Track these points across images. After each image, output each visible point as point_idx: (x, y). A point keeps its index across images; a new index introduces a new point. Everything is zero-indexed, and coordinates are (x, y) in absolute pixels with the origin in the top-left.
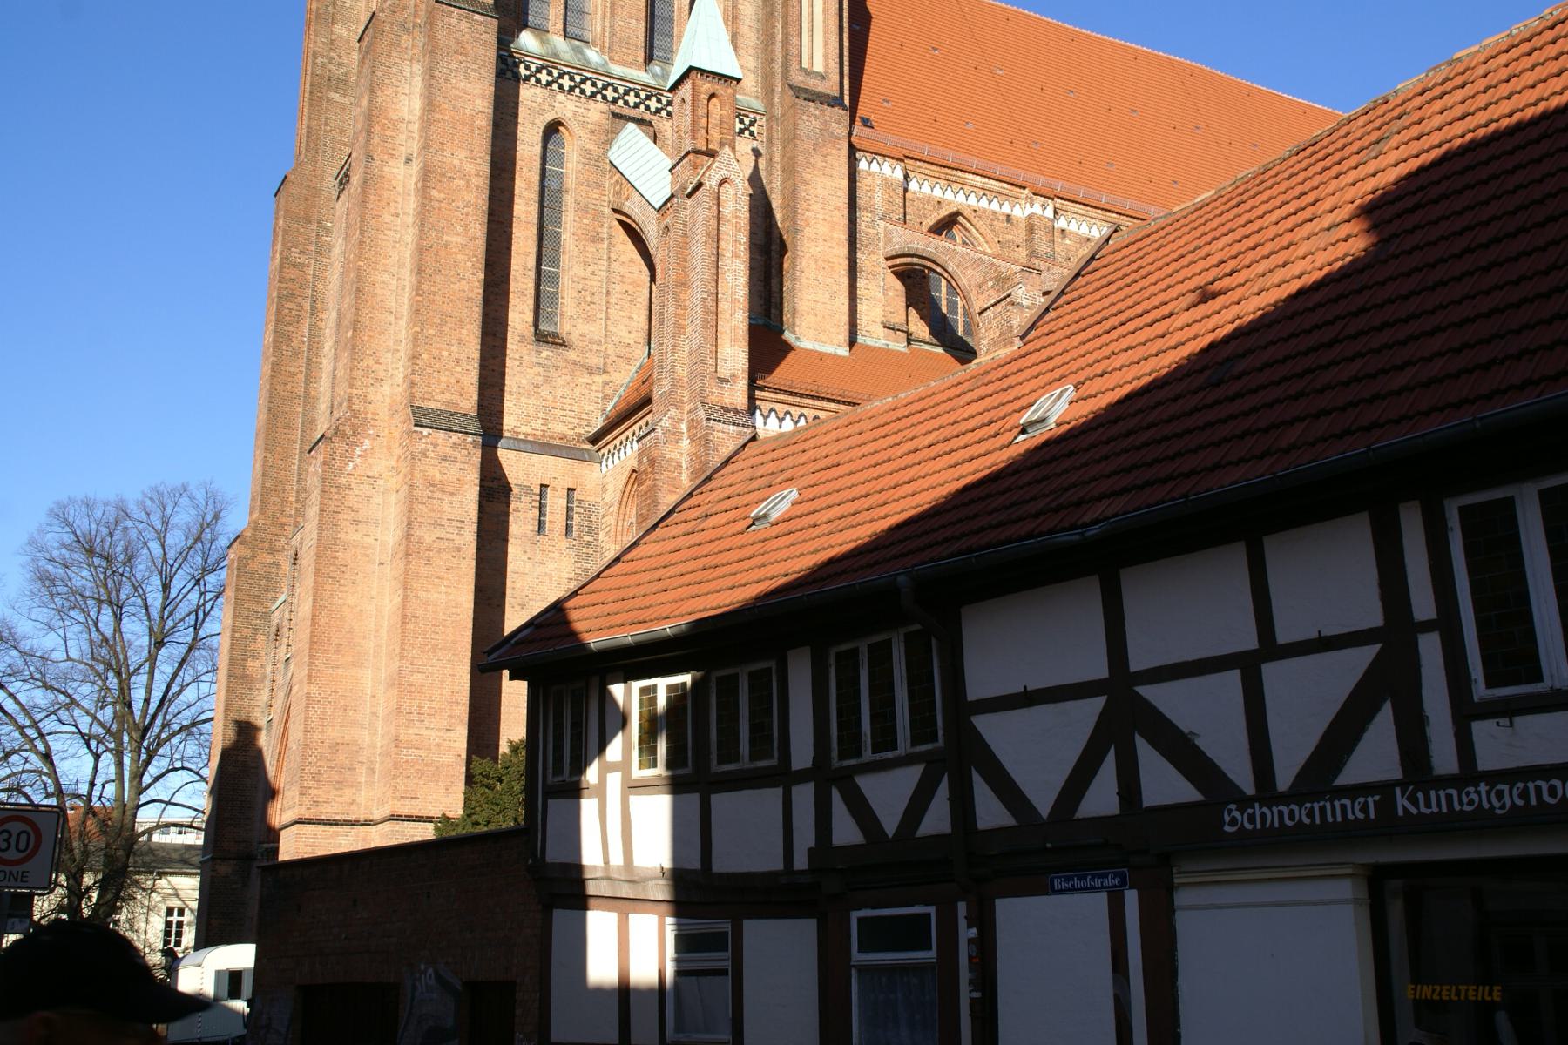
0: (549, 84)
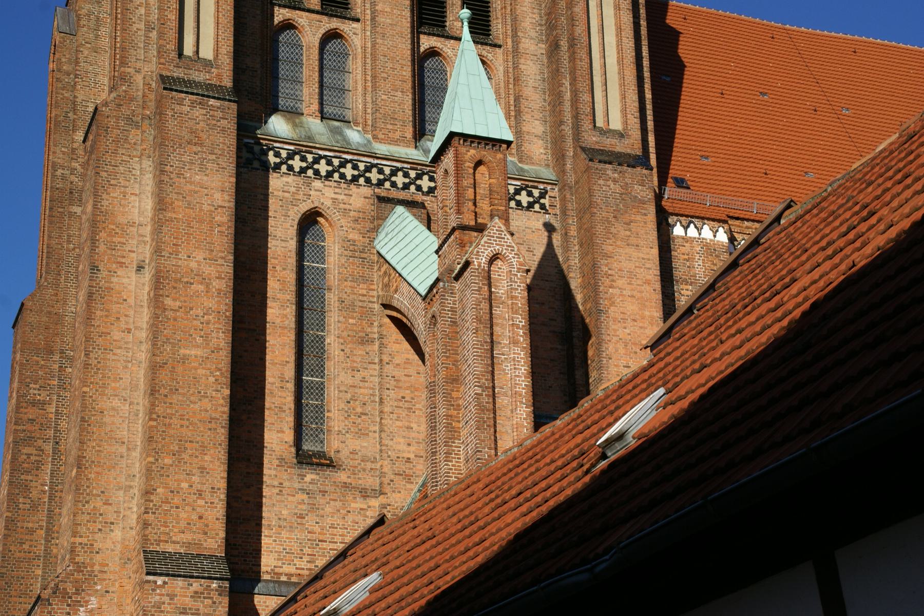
0: (303, 171)
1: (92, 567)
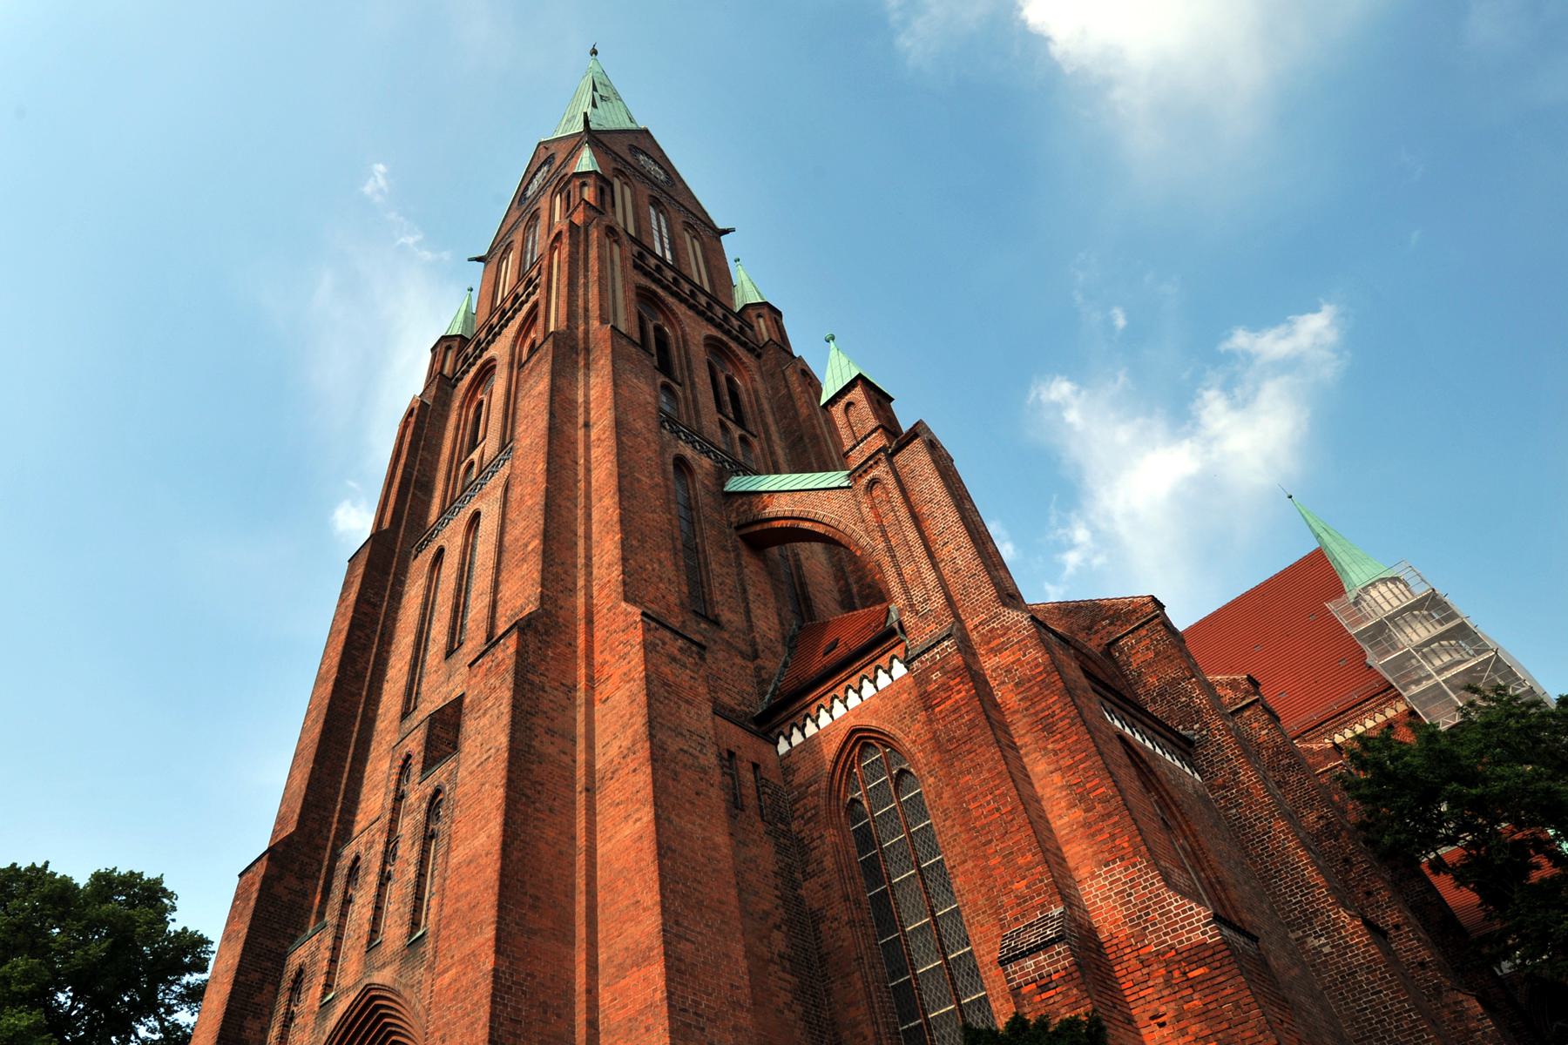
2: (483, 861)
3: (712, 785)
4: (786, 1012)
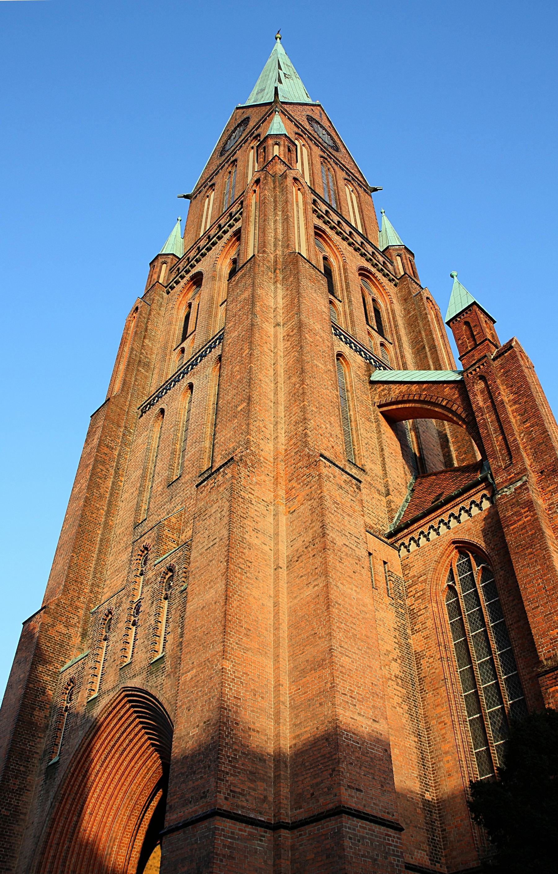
1: (260, 456)
2: (213, 607)
3: (363, 568)
4: (397, 708)
